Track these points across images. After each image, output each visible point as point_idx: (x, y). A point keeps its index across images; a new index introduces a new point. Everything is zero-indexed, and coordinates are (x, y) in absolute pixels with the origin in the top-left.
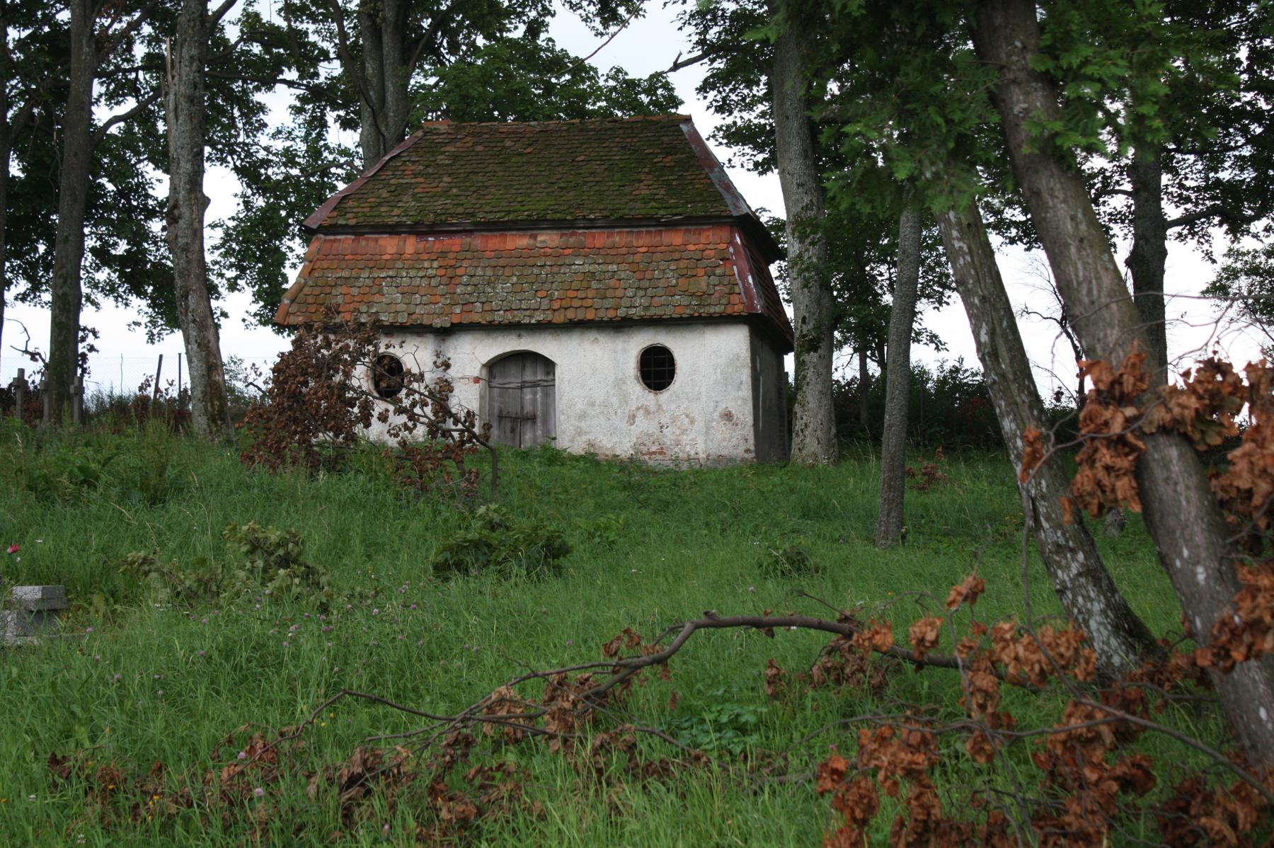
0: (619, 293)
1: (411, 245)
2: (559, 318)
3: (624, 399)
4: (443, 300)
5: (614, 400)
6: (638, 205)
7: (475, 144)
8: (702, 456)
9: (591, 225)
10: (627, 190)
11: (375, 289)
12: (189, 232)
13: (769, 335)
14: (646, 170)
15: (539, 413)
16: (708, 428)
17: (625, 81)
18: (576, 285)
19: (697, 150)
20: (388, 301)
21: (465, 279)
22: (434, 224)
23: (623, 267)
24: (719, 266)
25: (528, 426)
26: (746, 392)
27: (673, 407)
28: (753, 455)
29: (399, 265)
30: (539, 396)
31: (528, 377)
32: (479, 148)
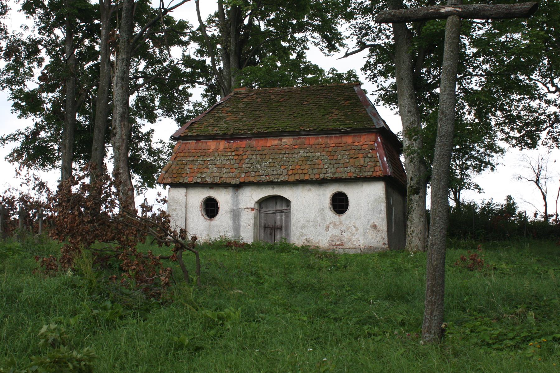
0: (321, 166)
1: (222, 145)
2: (291, 179)
3: (324, 218)
4: (236, 171)
5: (319, 219)
6: (331, 124)
7: (257, 98)
8: (362, 246)
9: (308, 134)
10: (326, 117)
11: (204, 166)
12: (120, 140)
13: (396, 185)
14: (336, 108)
15: (284, 225)
16: (365, 233)
17: (337, 74)
18: (300, 163)
19: (361, 98)
20: (210, 171)
21: (247, 160)
22: (233, 134)
23: (324, 153)
24: (370, 152)
25: (279, 231)
26: (384, 215)
27: (348, 222)
28: (387, 246)
29: (216, 154)
30: (283, 217)
31: (278, 208)
32: (259, 100)
